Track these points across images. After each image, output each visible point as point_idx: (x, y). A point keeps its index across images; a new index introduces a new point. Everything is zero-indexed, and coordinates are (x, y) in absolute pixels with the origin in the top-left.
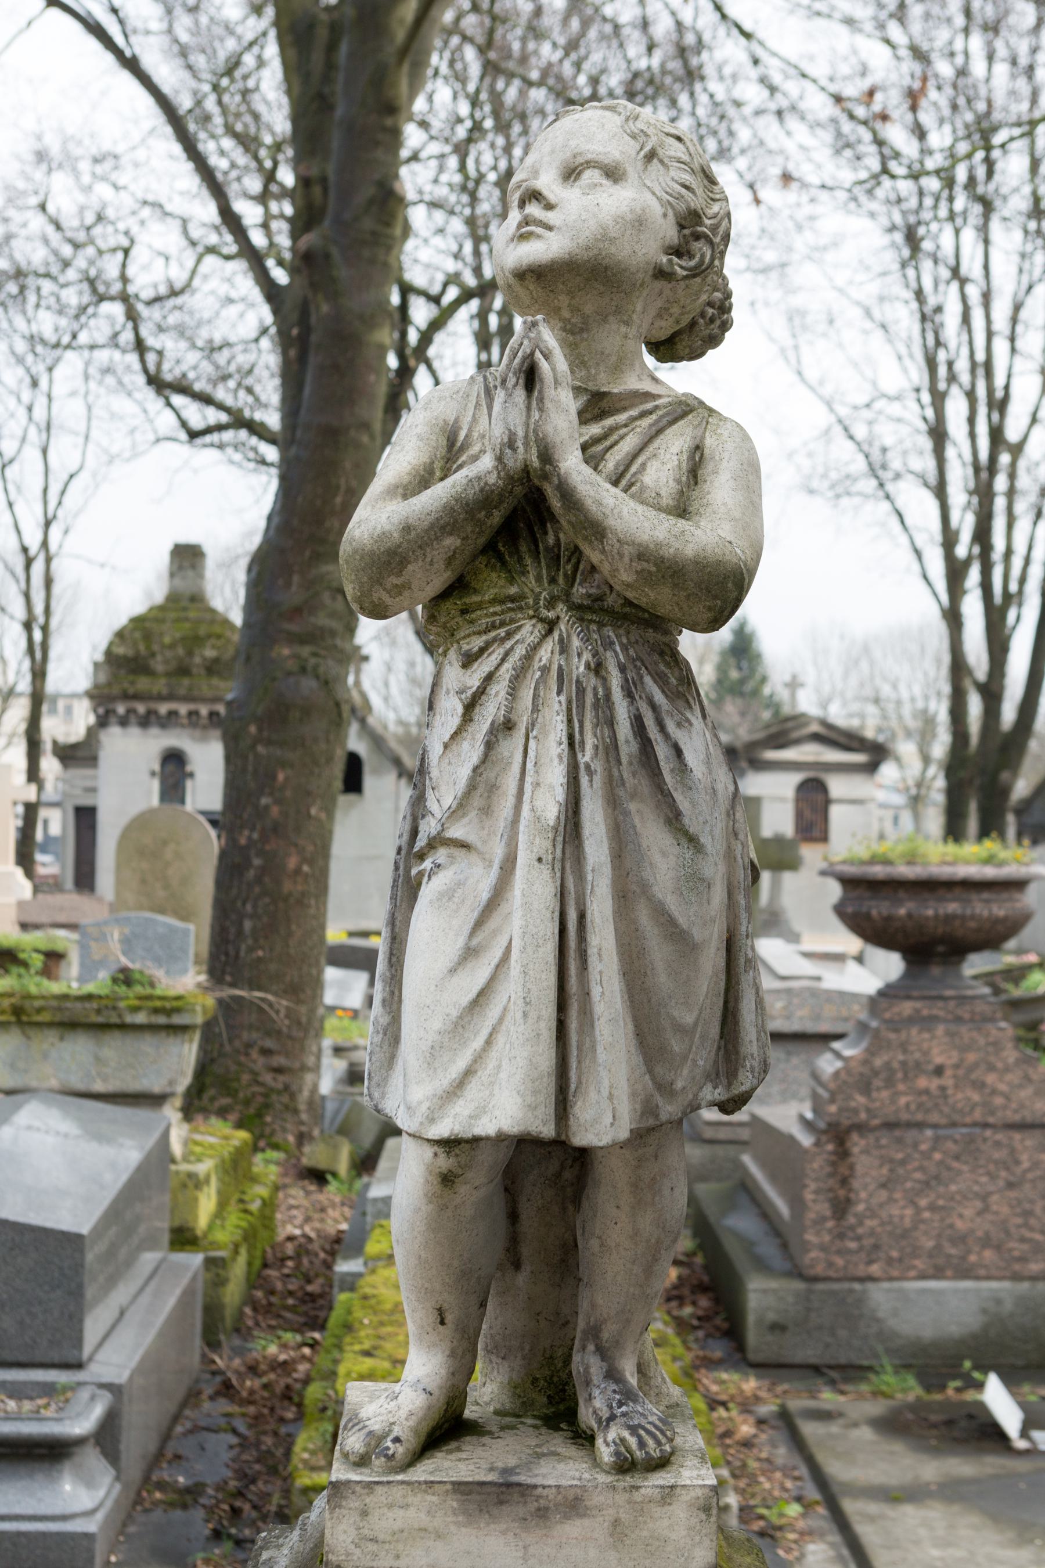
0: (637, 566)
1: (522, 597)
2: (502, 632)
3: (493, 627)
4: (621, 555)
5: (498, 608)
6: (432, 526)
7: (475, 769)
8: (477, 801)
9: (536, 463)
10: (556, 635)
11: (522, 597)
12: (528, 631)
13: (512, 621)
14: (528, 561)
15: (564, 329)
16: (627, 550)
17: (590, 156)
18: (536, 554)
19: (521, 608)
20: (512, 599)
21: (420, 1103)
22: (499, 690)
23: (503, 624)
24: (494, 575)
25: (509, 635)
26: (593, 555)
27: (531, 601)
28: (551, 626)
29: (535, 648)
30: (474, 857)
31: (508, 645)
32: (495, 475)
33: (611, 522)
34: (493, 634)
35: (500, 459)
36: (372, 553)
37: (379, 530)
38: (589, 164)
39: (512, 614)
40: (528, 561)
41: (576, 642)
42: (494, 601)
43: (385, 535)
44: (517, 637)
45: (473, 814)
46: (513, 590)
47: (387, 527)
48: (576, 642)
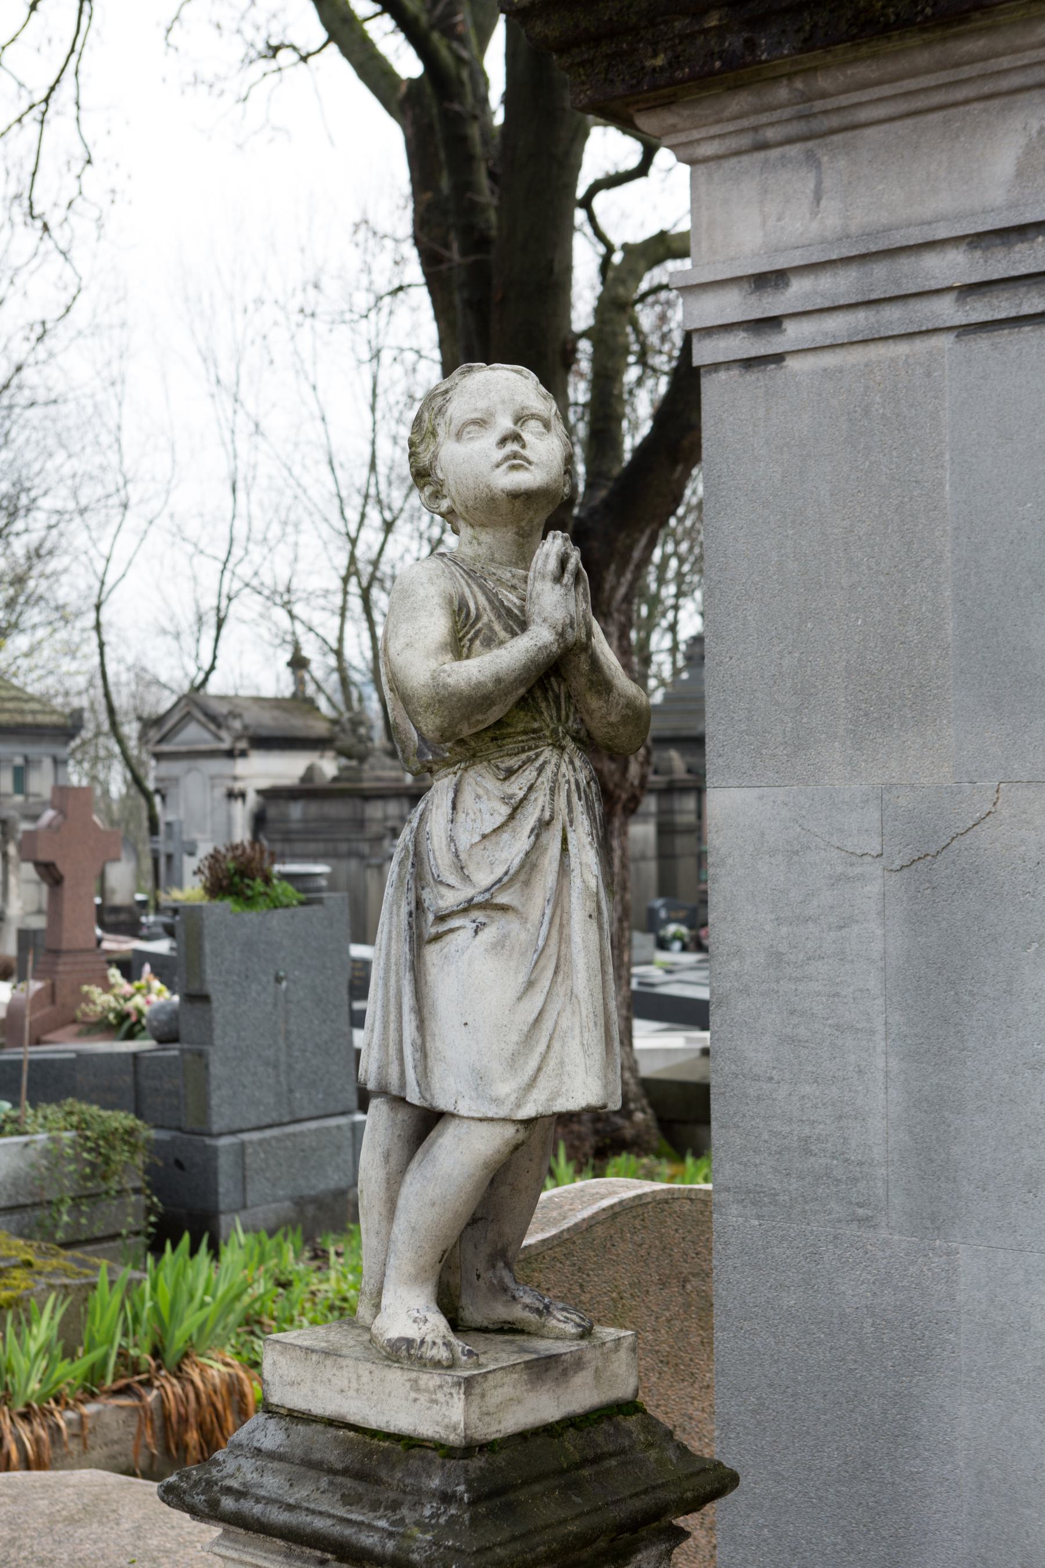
0: (624, 712)
1: (541, 730)
2: (531, 753)
3: (523, 751)
4: (618, 704)
5: (524, 738)
6: (516, 679)
7: (527, 854)
8: (522, 877)
9: (583, 636)
10: (566, 757)
11: (541, 730)
12: (548, 754)
13: (537, 747)
14: (543, 705)
15: (517, 533)
16: (622, 701)
17: (534, 411)
18: (546, 699)
19: (540, 738)
20: (534, 731)
21: (508, 1095)
22: (541, 798)
23: (530, 749)
24: (522, 713)
25: (538, 755)
26: (594, 703)
27: (548, 734)
28: (562, 748)
29: (558, 766)
30: (511, 916)
31: (537, 764)
32: (556, 645)
33: (616, 682)
34: (524, 756)
35: (562, 635)
36: (469, 698)
37: (474, 680)
38: (533, 416)
39: (531, 743)
40: (543, 705)
41: (578, 763)
42: (525, 732)
43: (479, 685)
44: (541, 759)
45: (517, 886)
46: (536, 725)
47: (482, 679)
48: (578, 763)
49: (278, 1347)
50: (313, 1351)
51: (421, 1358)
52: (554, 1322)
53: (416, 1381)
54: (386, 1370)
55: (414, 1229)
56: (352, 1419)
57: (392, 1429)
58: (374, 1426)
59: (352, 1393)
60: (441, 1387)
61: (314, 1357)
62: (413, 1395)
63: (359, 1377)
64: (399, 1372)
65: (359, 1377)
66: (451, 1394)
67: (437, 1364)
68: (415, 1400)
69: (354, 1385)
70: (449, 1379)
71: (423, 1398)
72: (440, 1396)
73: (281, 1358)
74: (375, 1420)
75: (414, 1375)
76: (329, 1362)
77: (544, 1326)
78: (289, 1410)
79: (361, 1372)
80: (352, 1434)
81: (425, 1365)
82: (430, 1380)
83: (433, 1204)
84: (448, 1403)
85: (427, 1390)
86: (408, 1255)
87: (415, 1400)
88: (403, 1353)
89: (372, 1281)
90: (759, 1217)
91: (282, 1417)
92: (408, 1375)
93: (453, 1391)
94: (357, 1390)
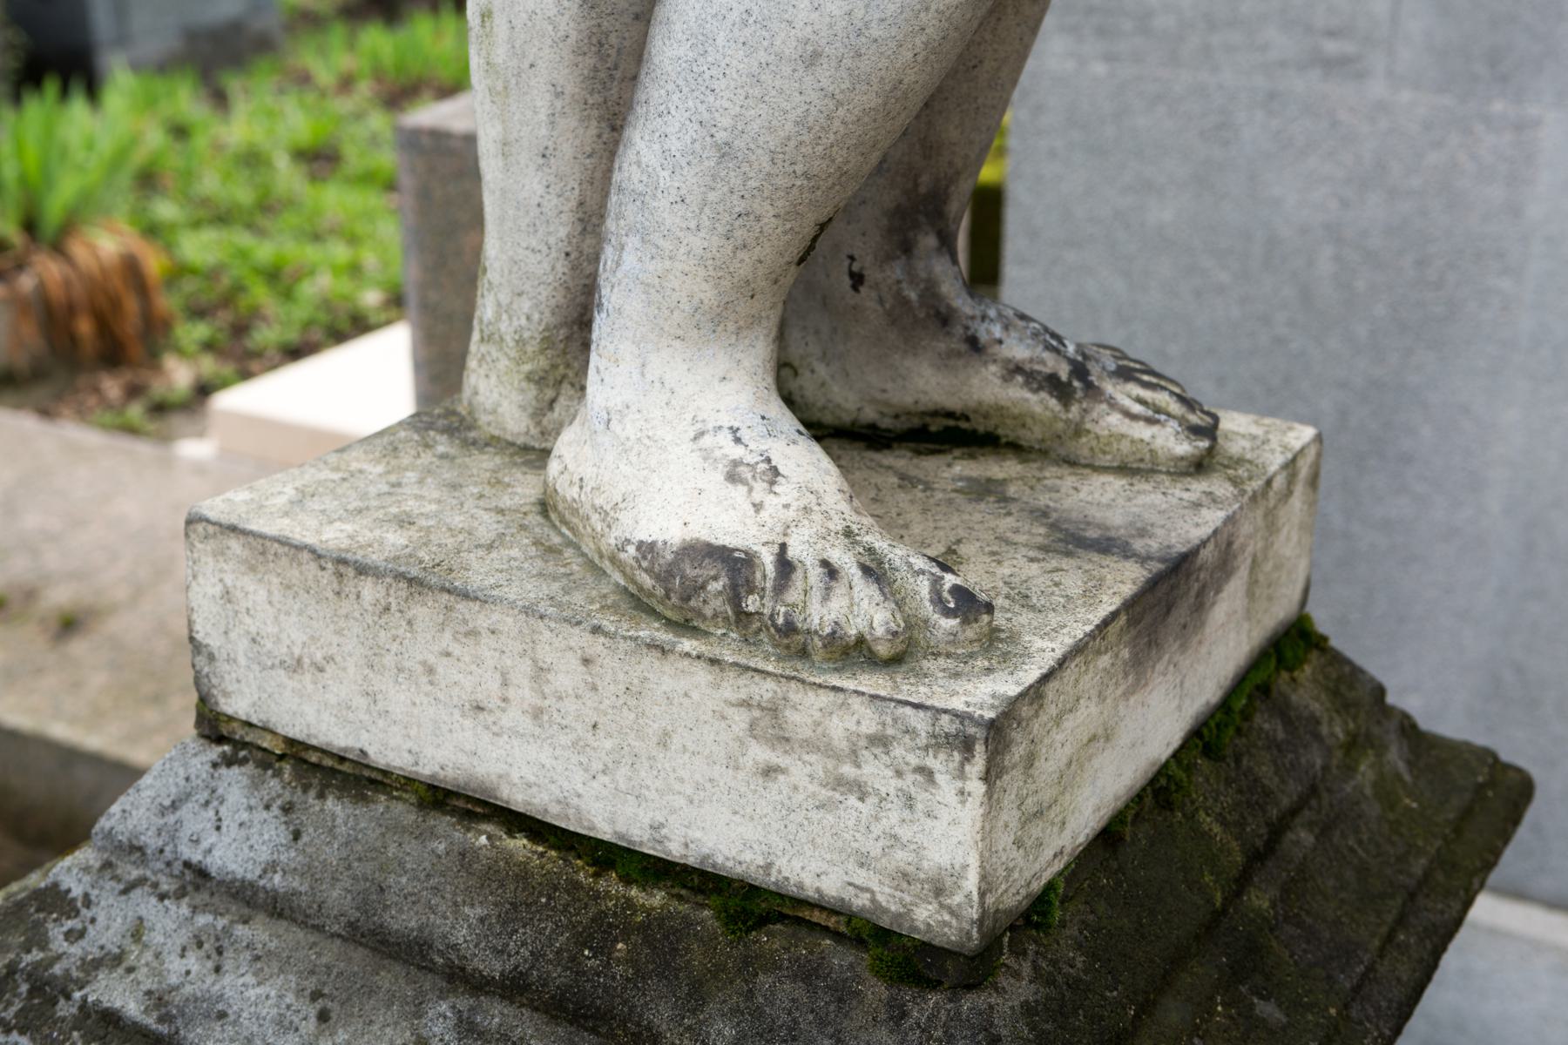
49: (235, 545)
50: (362, 570)
51: (790, 629)
52: (1115, 420)
53: (773, 710)
54: (650, 659)
55: (725, 152)
56: (517, 798)
57: (674, 850)
58: (605, 832)
59: (514, 717)
60: (880, 741)
61: (370, 590)
62: (760, 753)
63: (540, 672)
64: (702, 675)
65: (540, 672)
66: (927, 773)
67: (852, 652)
68: (769, 772)
69: (523, 693)
70: (919, 721)
71: (802, 771)
72: (874, 771)
73: (248, 583)
74: (605, 814)
75: (765, 690)
76: (424, 612)
77: (1078, 431)
78: (291, 742)
79: (546, 655)
80: (519, 844)
81: (803, 653)
82: (836, 710)
83: (812, 59)
84: (909, 803)
85: (818, 745)
86: (697, 242)
87: (769, 772)
88: (700, 598)
89: (526, 305)
90: (1110, 58)
91: (267, 761)
92: (735, 687)
93: (934, 762)
94: (537, 713)
